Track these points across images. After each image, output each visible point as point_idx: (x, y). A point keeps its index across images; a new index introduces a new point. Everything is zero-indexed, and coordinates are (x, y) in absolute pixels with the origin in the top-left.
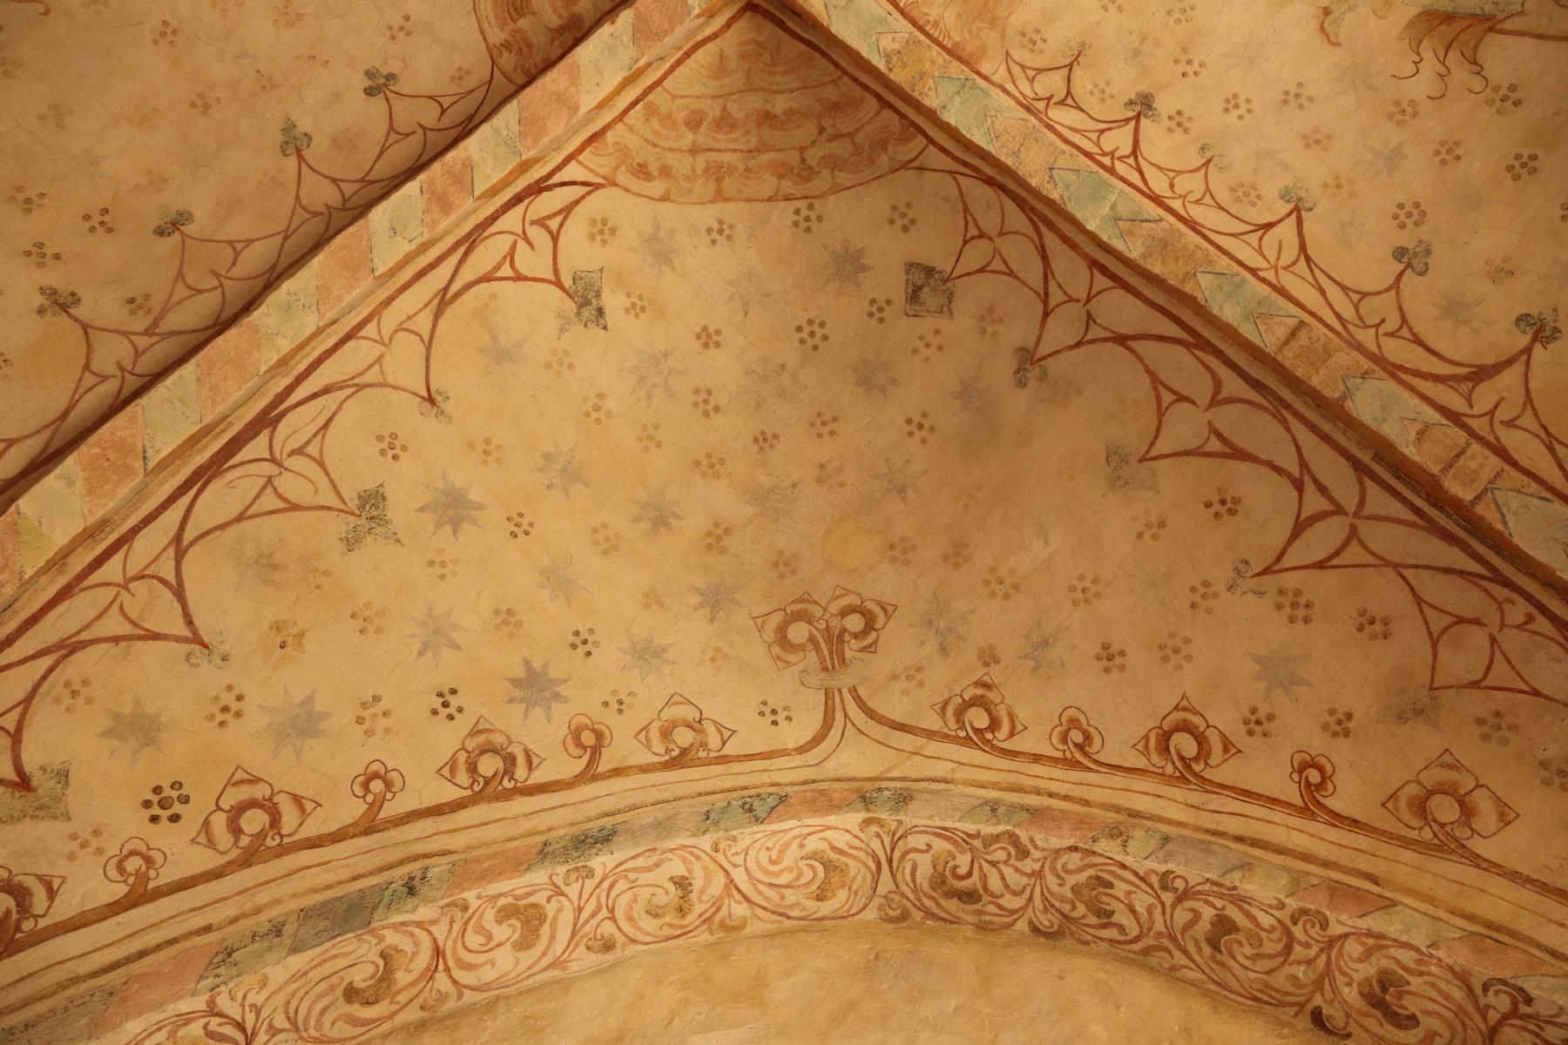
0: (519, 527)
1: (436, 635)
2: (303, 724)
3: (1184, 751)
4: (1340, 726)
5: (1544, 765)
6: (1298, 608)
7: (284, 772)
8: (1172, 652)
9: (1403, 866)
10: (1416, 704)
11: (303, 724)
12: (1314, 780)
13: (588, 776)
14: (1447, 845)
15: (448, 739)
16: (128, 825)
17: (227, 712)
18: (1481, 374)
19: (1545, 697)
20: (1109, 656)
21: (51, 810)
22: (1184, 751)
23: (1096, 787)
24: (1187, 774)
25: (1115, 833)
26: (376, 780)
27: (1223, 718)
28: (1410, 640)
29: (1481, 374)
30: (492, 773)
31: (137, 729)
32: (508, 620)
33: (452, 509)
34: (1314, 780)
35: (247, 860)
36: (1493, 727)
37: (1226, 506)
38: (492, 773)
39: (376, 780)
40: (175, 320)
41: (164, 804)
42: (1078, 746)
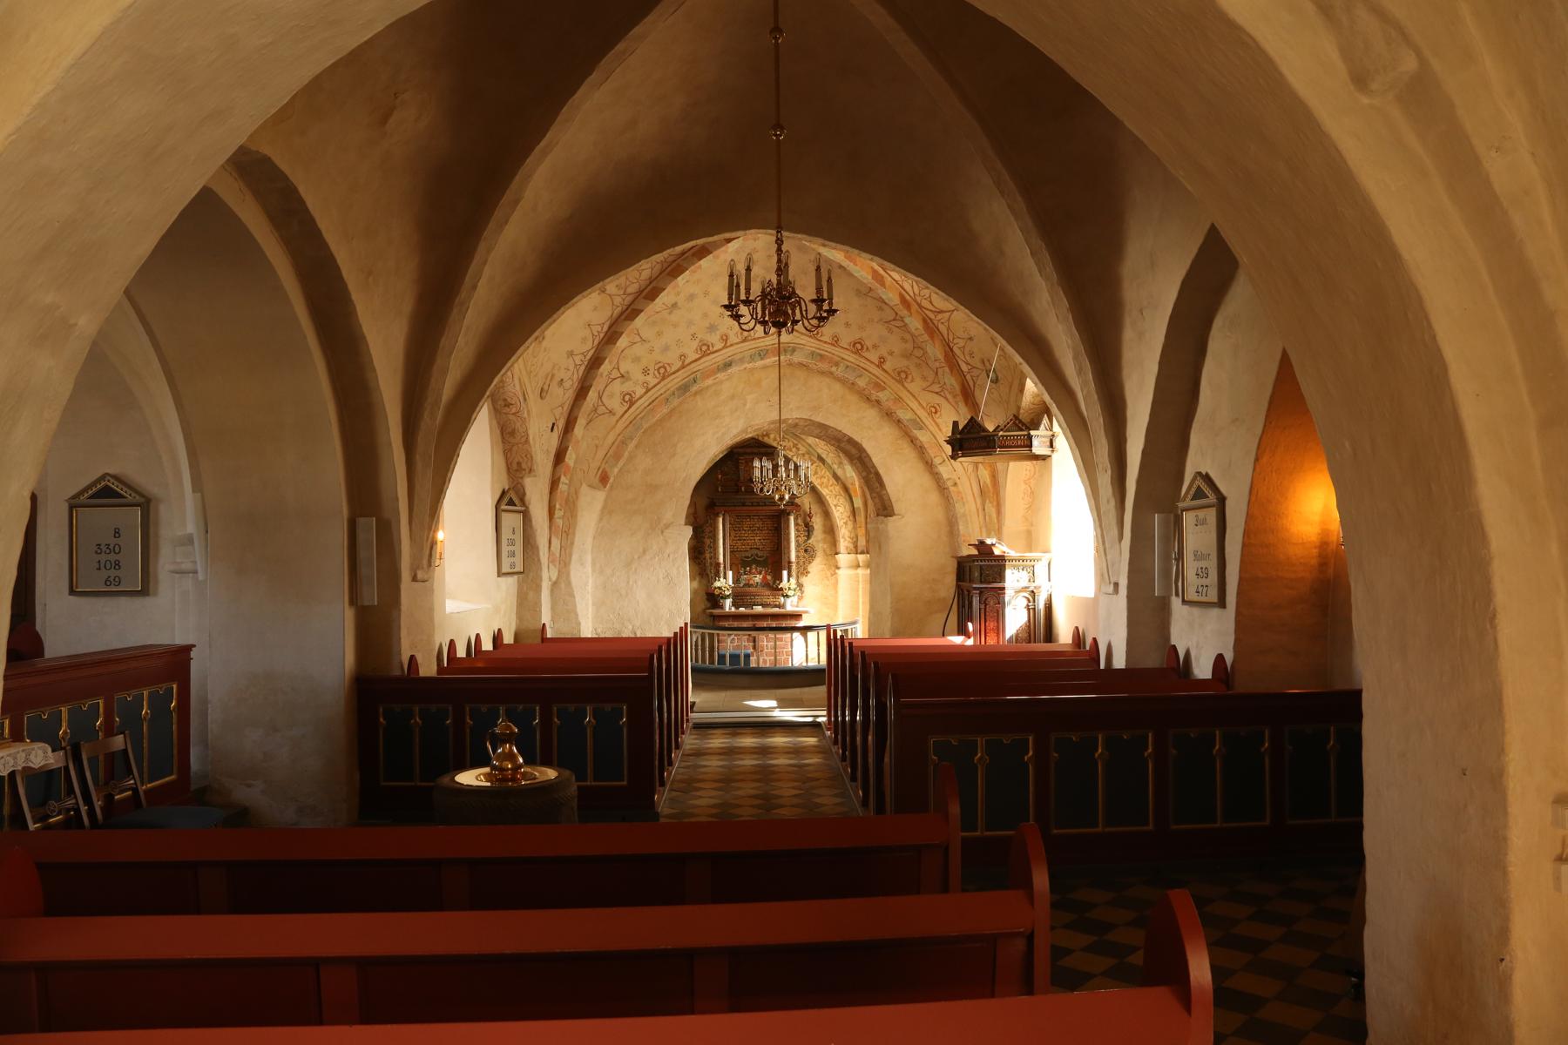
0: (706, 294)
1: (690, 323)
2: (666, 349)
3: (858, 347)
4: (891, 353)
6: (890, 331)
7: (665, 359)
8: (862, 328)
9: (890, 382)
10: (907, 355)
11: (666, 349)
12: (882, 361)
13: (725, 347)
14: (900, 382)
15: (695, 344)
16: (641, 378)
17: (651, 351)
18: (941, 312)
20: (847, 324)
21: (629, 379)
22: (858, 347)
23: (837, 351)
24: (857, 352)
25: (837, 364)
26: (683, 356)
27: (868, 343)
28: (909, 346)
29: (941, 312)
30: (705, 350)
31: (637, 360)
32: (705, 315)
33: (691, 297)
34: (882, 361)
35: (663, 378)
36: (918, 366)
37: (881, 309)
38: (705, 350)
39: (683, 356)
40: (630, 290)
41: (645, 372)
42: (835, 341)
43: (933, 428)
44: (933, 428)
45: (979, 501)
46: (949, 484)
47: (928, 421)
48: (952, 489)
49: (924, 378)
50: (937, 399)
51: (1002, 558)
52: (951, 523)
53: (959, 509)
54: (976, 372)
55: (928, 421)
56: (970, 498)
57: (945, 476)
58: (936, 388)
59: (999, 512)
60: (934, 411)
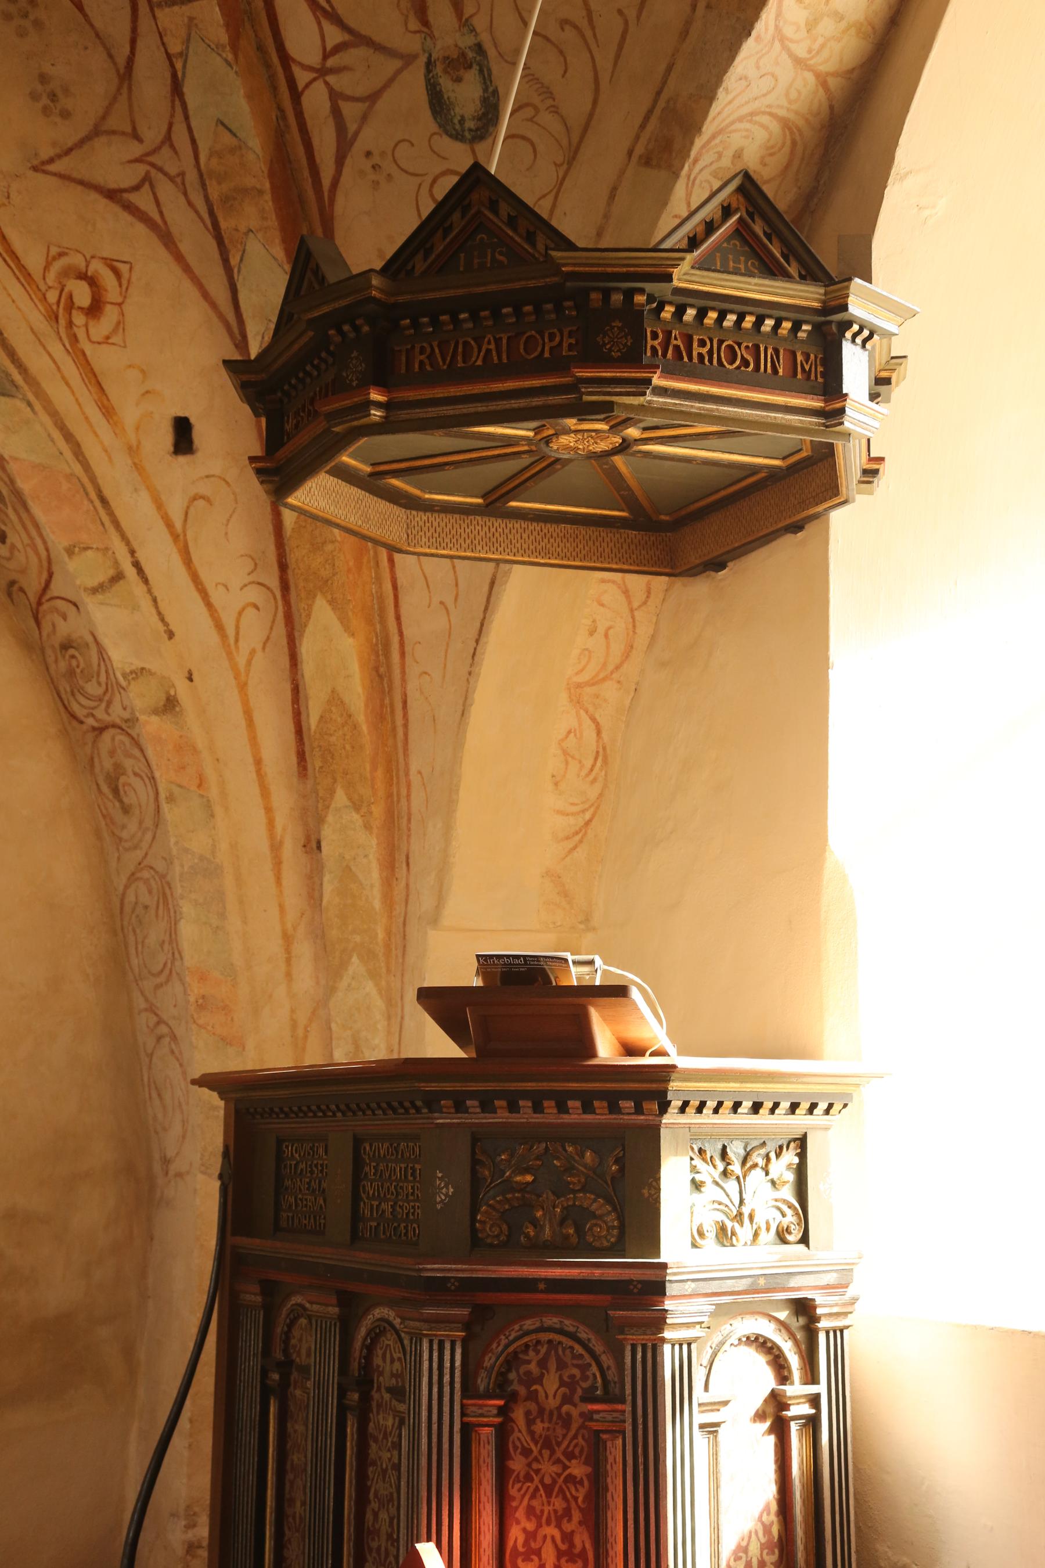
5: (43, 79)
19: (85, 15)
43: (68, 394)
44: (68, 394)
45: (284, 800)
46: (140, 698)
47: (45, 358)
48: (151, 726)
49: (50, 97)
50: (112, 234)
51: (648, 1089)
52: (128, 925)
53: (185, 832)
54: (359, 73)
55: (45, 358)
56: (241, 782)
57: (121, 656)
58: (112, 163)
59: (395, 859)
60: (84, 300)
